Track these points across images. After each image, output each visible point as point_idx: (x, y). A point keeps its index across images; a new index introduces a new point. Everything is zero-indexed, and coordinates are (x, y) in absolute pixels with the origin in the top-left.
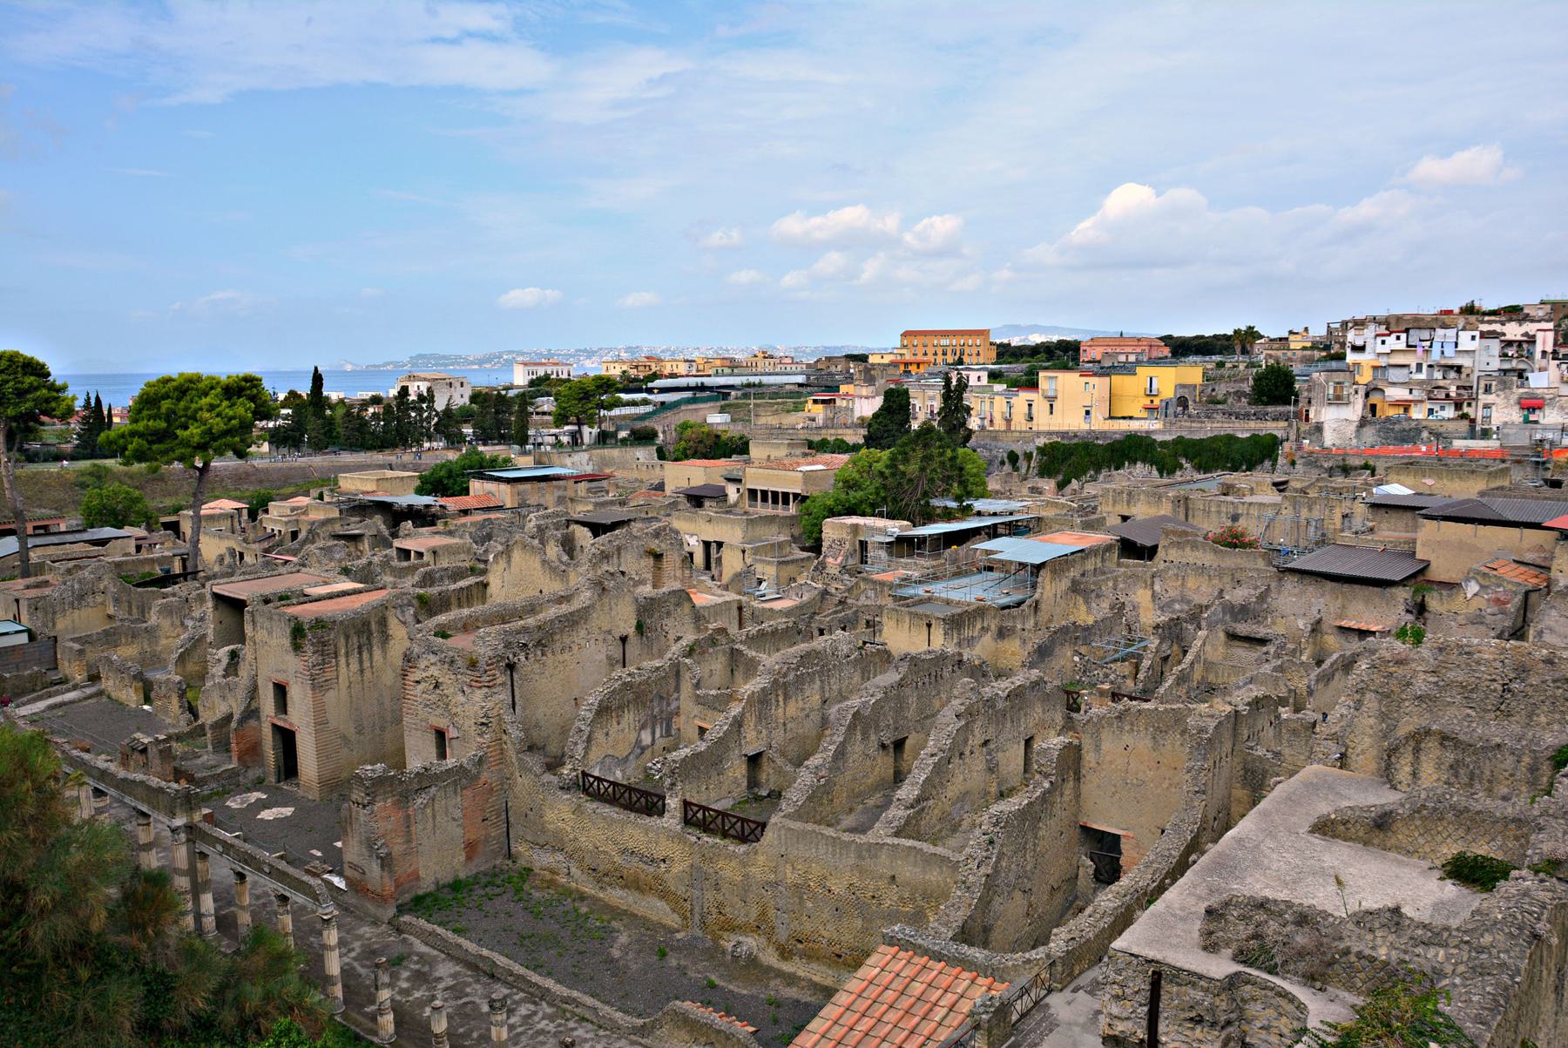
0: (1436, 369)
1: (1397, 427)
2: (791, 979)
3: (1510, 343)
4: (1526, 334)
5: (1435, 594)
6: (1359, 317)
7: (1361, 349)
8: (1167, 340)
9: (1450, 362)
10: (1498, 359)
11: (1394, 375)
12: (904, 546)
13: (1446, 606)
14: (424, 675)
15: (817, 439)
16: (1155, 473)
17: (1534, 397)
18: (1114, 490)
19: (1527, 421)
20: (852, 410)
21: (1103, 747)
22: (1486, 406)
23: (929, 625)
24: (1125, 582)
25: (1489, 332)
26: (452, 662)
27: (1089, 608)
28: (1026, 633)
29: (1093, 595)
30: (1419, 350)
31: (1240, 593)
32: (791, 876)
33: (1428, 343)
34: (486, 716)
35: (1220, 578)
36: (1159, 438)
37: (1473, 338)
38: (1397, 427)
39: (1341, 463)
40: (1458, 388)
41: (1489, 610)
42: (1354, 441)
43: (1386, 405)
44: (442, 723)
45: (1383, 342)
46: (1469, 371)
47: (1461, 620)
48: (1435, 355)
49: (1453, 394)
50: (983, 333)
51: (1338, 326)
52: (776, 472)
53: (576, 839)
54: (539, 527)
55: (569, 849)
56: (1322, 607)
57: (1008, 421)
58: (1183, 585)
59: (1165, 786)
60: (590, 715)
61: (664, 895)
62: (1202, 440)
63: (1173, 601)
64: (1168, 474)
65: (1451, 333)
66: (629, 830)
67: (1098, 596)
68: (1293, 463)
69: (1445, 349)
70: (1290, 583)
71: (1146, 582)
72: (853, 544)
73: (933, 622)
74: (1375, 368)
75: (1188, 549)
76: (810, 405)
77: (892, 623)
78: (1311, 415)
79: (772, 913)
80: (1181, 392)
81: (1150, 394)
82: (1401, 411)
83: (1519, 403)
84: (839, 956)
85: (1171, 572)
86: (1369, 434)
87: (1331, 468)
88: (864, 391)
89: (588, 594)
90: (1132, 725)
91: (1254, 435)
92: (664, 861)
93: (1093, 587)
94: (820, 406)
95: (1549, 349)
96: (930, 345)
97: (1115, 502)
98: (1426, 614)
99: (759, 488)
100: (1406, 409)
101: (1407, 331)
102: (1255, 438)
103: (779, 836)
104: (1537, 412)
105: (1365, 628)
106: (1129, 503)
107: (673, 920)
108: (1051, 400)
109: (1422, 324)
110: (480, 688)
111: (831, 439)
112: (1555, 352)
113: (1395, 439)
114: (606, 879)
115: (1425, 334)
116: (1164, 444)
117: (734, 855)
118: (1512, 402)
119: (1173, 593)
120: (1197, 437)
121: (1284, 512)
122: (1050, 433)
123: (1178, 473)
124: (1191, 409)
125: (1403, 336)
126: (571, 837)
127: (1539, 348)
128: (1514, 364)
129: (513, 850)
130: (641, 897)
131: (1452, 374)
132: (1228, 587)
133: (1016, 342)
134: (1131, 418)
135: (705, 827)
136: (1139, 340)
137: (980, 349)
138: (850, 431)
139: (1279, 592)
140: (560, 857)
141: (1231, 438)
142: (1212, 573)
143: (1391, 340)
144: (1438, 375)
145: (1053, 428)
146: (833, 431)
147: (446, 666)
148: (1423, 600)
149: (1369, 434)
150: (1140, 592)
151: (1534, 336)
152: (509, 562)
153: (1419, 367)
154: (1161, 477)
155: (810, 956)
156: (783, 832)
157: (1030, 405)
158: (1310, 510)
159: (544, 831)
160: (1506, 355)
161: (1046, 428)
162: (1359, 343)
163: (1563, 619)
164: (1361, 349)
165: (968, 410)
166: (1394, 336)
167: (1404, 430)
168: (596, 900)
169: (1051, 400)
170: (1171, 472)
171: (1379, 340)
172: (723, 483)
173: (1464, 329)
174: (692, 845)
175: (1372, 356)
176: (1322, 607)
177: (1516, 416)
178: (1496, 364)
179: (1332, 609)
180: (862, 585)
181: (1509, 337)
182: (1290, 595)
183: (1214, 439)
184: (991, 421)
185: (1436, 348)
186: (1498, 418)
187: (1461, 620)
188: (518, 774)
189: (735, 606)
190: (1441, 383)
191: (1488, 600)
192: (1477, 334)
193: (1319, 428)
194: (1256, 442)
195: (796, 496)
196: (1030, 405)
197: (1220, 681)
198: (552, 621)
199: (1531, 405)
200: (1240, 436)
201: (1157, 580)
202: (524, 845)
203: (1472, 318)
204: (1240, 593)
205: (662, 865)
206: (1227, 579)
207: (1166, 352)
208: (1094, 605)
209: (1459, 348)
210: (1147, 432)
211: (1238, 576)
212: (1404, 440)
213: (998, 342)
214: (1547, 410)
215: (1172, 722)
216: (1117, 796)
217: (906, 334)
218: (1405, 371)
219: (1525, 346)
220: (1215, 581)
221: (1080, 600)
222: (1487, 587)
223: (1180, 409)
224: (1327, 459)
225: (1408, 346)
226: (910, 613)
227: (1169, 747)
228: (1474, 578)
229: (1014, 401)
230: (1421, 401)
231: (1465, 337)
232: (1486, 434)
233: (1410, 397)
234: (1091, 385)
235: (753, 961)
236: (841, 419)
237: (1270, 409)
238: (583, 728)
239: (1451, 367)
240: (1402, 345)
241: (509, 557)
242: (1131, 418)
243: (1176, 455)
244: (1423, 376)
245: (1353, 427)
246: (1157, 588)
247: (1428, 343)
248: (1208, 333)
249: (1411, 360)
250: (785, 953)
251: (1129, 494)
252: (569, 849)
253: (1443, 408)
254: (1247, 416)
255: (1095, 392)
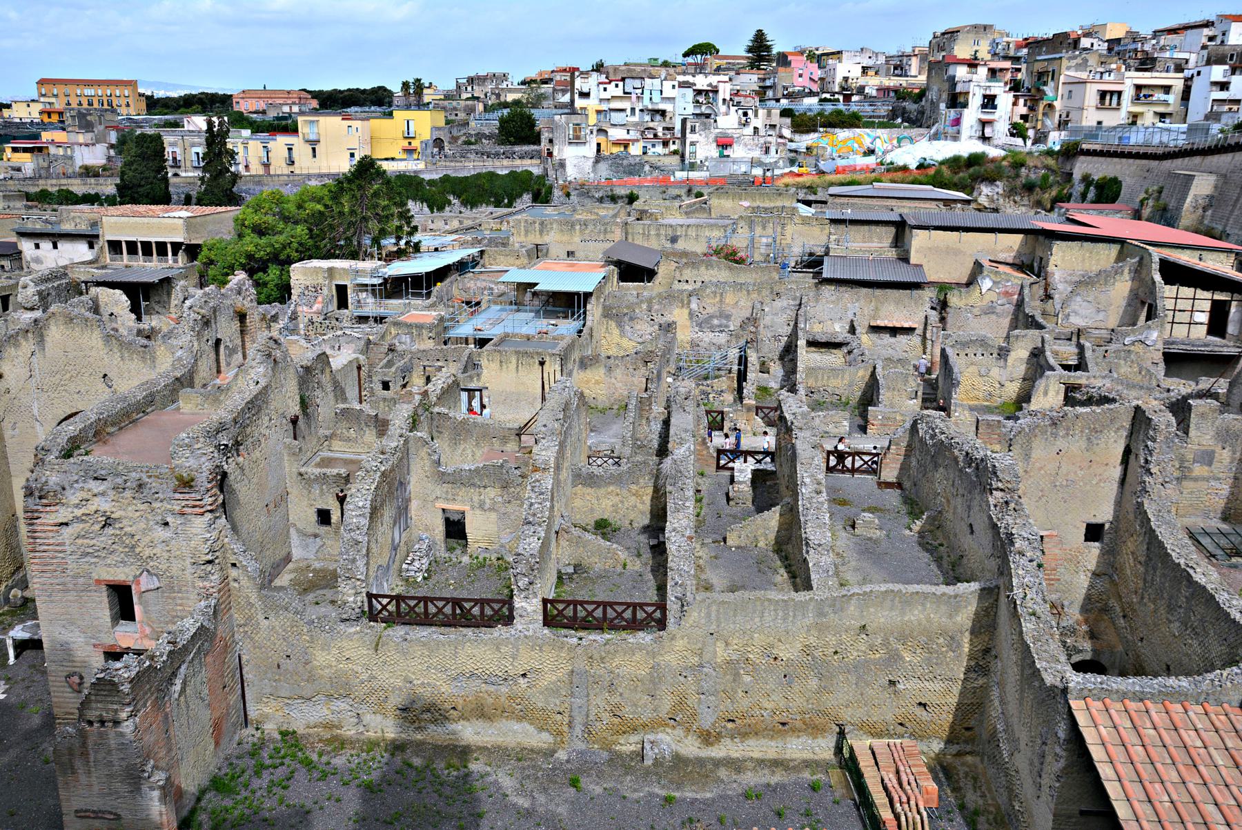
0: (646, 112)
1: (625, 162)
2: (736, 765)
3: (699, 92)
4: (710, 85)
5: (956, 292)
6: (482, 73)
7: (585, 95)
8: (316, 95)
9: (656, 107)
10: (692, 105)
11: (616, 118)
12: (395, 287)
13: (964, 302)
14: (78, 512)
15: (33, 190)
16: (426, 209)
17: (726, 136)
18: (526, 221)
19: (722, 156)
20: (71, 158)
21: (1033, 455)
22: (693, 144)
23: (542, 363)
24: (660, 303)
25: (685, 82)
26: (140, 486)
27: (623, 333)
28: (612, 361)
29: (626, 318)
30: (634, 96)
31: (780, 304)
32: (721, 653)
33: (640, 91)
34: (212, 551)
35: (759, 292)
36: (427, 177)
37: (674, 87)
38: (625, 162)
39: (610, 194)
40: (664, 129)
41: (999, 302)
42: (592, 175)
43: (610, 144)
44: (121, 575)
45: (605, 89)
46: (671, 115)
47: (977, 312)
48: (646, 102)
49: (660, 134)
50: (132, 84)
51: (465, 81)
52: (146, 220)
53: (372, 678)
54: (40, 293)
55: (360, 691)
56: (857, 310)
57: (267, 165)
58: (721, 301)
59: (1094, 482)
60: (365, 522)
61: (523, 715)
62: (466, 178)
63: (711, 317)
64: (438, 210)
65: (657, 82)
66: (469, 649)
67: (631, 319)
68: (568, 195)
69: (653, 96)
70: (828, 290)
71: (682, 301)
72: (330, 290)
73: (547, 359)
74: (599, 112)
75: (703, 269)
76: (8, 153)
77: (494, 366)
78: (555, 153)
79: (692, 700)
80: (437, 134)
81: (408, 137)
82: (622, 149)
83: (717, 141)
84: (783, 724)
85: (708, 291)
86: (604, 168)
87: (602, 198)
88: (81, 138)
89: (261, 369)
90: (1068, 429)
91: (512, 172)
92: (524, 675)
93: (625, 311)
94: (27, 156)
95: (728, 98)
96: (73, 95)
97: (527, 232)
98: (948, 309)
99: (123, 238)
100: (626, 146)
101: (623, 79)
102: (513, 174)
103: (708, 615)
104: (729, 148)
105: (898, 325)
106: (541, 232)
107: (541, 740)
108: (313, 144)
109: (635, 75)
110: (202, 514)
111: (54, 190)
112: (731, 99)
113: (624, 172)
114: (427, 716)
115: (637, 83)
116: (432, 183)
117: (640, 647)
118: (711, 140)
119: (710, 310)
120: (461, 175)
121: (740, 231)
122: (321, 176)
123: (447, 209)
124: (447, 149)
125: (621, 84)
126: (365, 677)
127: (721, 96)
128: (704, 109)
129: (253, 713)
130: (487, 725)
131: (658, 117)
132: (768, 300)
133: (160, 94)
134: (393, 159)
135: (577, 624)
136: (289, 92)
137: (130, 100)
138: (78, 181)
139: (817, 301)
140: (342, 705)
141: (492, 176)
142: (750, 288)
143: (611, 87)
144: (647, 118)
145: (324, 171)
146: (54, 182)
147: (128, 494)
148: (945, 298)
149: (604, 168)
150: (677, 311)
151: (716, 87)
152: (41, 341)
153: (633, 110)
154: (432, 212)
155: (744, 734)
156: (714, 608)
157: (290, 149)
158: (764, 228)
159: (311, 679)
160: (698, 102)
161: (317, 171)
162: (585, 90)
163: (1085, 303)
164: (585, 95)
165: (232, 154)
166: (613, 84)
167: (631, 165)
168: (420, 744)
169: (313, 144)
170: (441, 209)
171: (602, 87)
172: (14, 239)
173: (666, 79)
174: (572, 649)
175: (597, 102)
176: (857, 310)
177: (714, 152)
178: (691, 109)
179: (866, 312)
180: (393, 331)
181: (699, 87)
182: (828, 302)
183: (479, 176)
184: (247, 167)
185: (647, 93)
186: (700, 156)
187: (977, 312)
188: (261, 617)
189: (355, 365)
190: (651, 125)
191: (999, 294)
192: (676, 83)
193: (562, 165)
194: (515, 178)
195: (176, 247)
196: (290, 149)
197: (819, 384)
198: (243, 410)
199: (724, 144)
200: (500, 173)
201: (694, 299)
202: (273, 703)
203: (671, 70)
204: (780, 304)
205: (521, 680)
206: (765, 292)
207: (315, 104)
208: (627, 327)
209: (664, 96)
210: (415, 172)
211: (776, 289)
212: (631, 173)
213: (149, 93)
214: (735, 146)
215: (1109, 422)
216: (1044, 500)
217: (42, 82)
218: (622, 114)
219: (711, 95)
220: (755, 296)
221: (613, 324)
222: (999, 282)
223: (436, 150)
224: (597, 190)
225: (625, 93)
226: (517, 353)
227: (1103, 446)
228: (988, 276)
229: (271, 145)
230: (637, 140)
231: (668, 85)
232: (692, 167)
233: (628, 137)
234: (354, 128)
235: (679, 761)
236: (58, 168)
237: (517, 148)
238: (360, 538)
239: (657, 111)
240: (619, 92)
241: (42, 336)
242: (393, 159)
243: (444, 193)
244: (636, 119)
245: (590, 163)
246: (694, 306)
247: (640, 91)
248: (343, 87)
249: (626, 105)
250: (708, 738)
251: (542, 224)
252: (360, 691)
253: (654, 146)
254: (497, 155)
255: (360, 133)
